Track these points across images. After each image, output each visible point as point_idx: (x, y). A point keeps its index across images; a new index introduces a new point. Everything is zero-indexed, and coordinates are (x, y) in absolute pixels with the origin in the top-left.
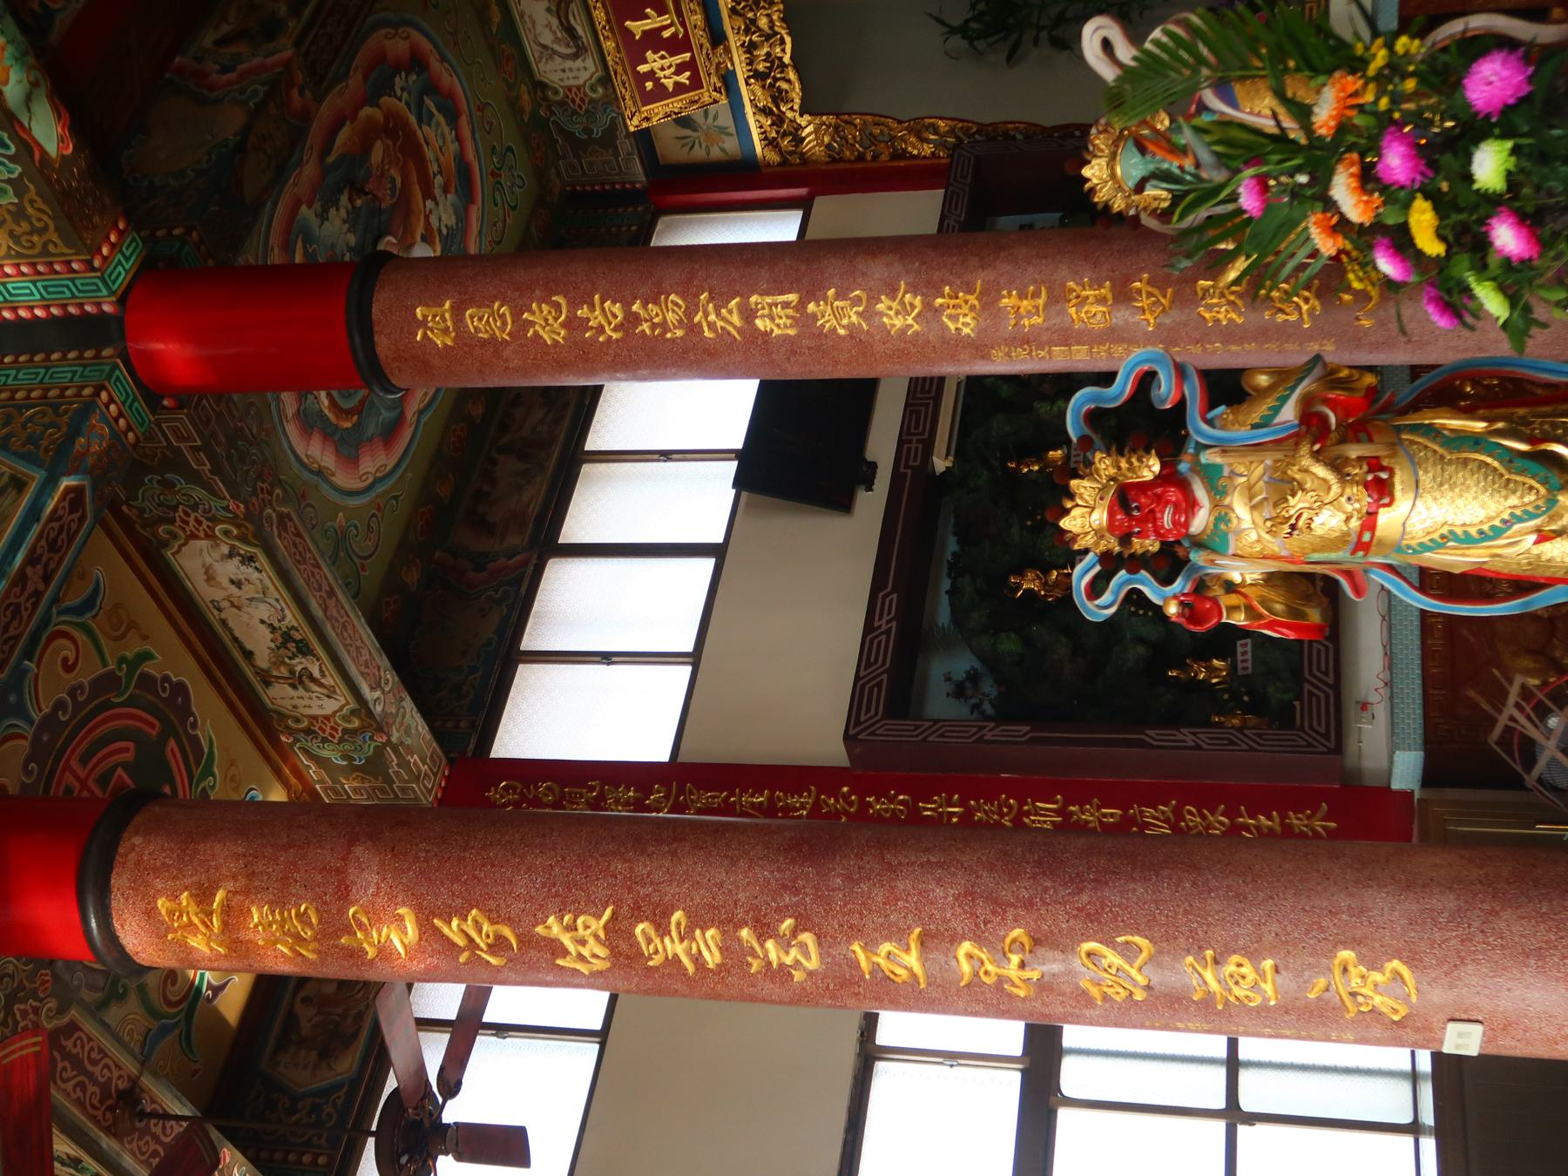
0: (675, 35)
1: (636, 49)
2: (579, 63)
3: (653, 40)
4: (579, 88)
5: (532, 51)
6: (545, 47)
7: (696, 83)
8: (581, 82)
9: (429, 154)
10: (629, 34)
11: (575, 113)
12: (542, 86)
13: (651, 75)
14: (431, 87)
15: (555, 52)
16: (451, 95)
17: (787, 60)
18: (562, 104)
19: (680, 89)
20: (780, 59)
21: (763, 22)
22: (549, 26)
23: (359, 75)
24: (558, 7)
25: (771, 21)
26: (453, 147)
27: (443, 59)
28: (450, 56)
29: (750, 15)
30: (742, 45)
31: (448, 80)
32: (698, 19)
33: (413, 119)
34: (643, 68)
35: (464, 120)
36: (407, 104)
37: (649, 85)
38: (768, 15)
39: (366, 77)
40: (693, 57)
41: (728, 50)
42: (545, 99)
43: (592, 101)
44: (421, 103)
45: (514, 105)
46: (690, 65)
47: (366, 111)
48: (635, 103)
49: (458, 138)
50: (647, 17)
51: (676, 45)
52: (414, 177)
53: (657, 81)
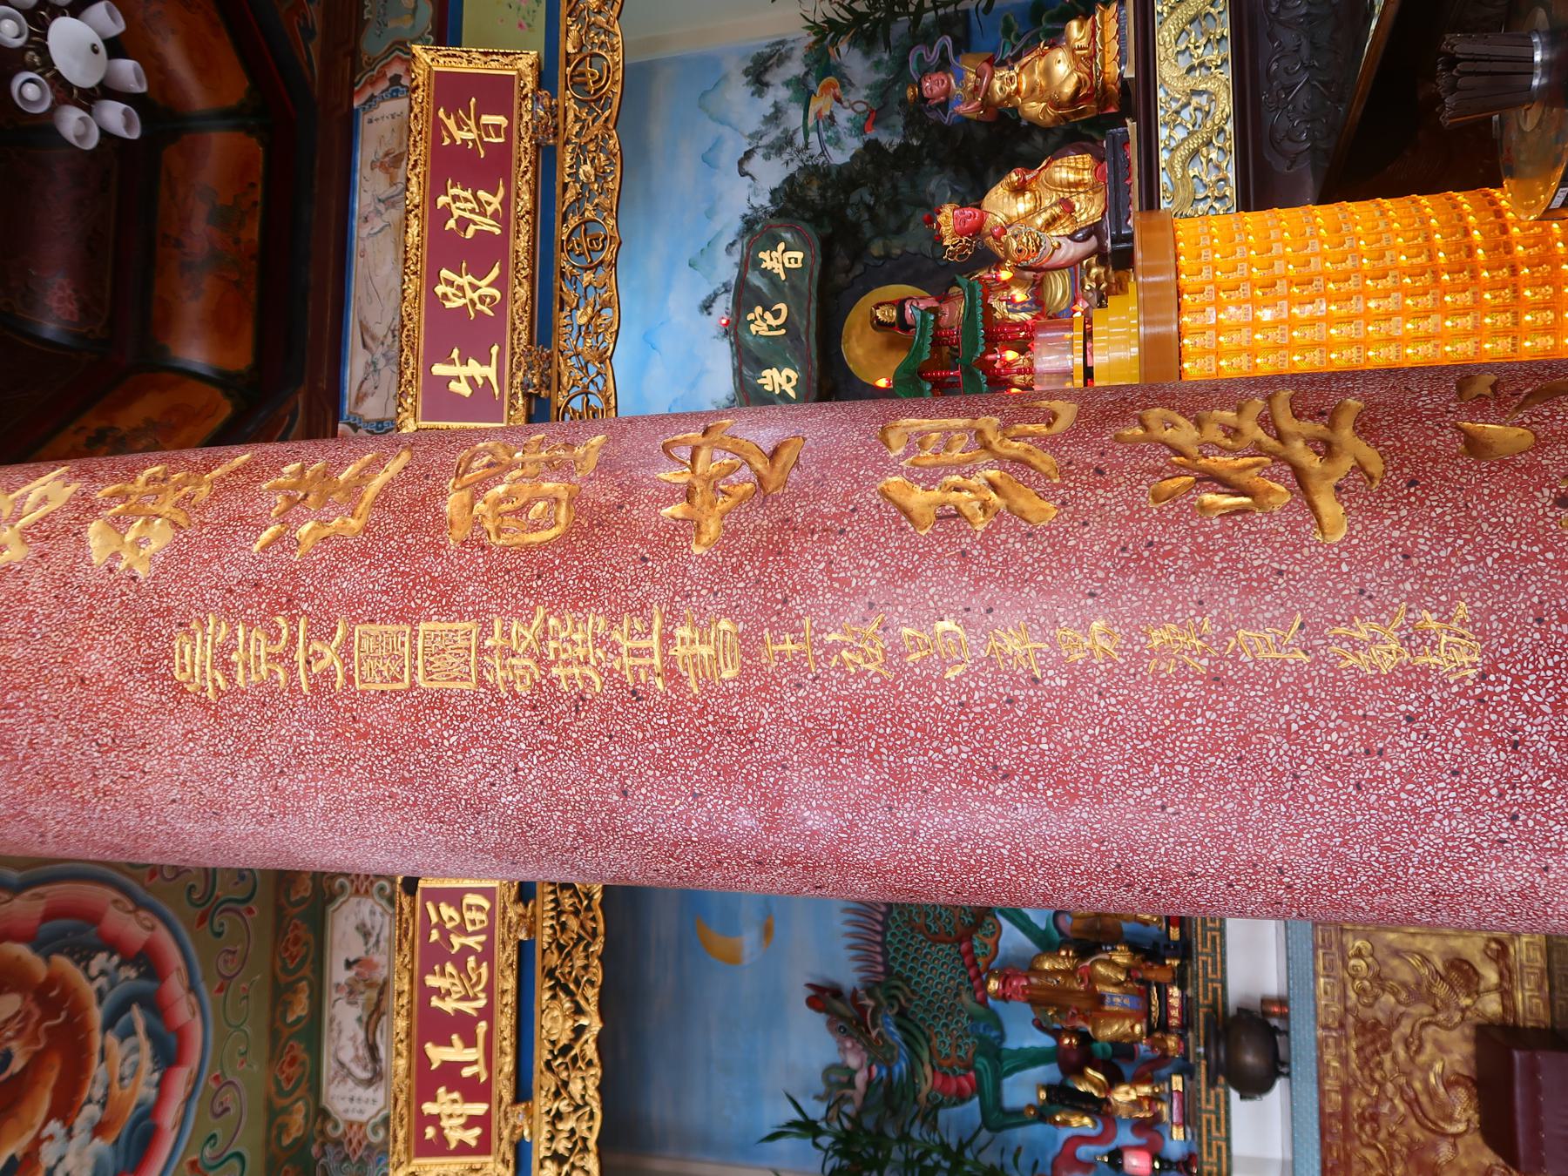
0: (476, 1077)
1: (428, 1080)
2: (369, 1093)
3: (450, 1073)
4: (361, 1125)
5: (328, 1066)
6: (342, 1065)
7: (484, 1147)
8: (364, 1118)
9: (98, 1070)
10: (424, 1060)
11: (347, 1158)
12: (323, 1114)
13: (435, 1120)
14: (156, 1006)
15: (350, 1074)
16: (181, 1034)
17: (592, 1144)
18: (338, 1143)
19: (463, 1149)
20: (585, 1140)
21: (576, 1088)
22: (353, 1039)
23: (40, 907)
24: (370, 1017)
25: (585, 1088)
26: (145, 1090)
27: (192, 988)
28: (203, 987)
29: (564, 1075)
30: (548, 1112)
31: (183, 1011)
32: (507, 1064)
33: (97, 1015)
34: (429, 1108)
35: (181, 1079)
36: (101, 994)
37: (430, 1132)
38: (583, 1079)
39: (48, 916)
40: (489, 1112)
41: (529, 1114)
42: (322, 1132)
43: (370, 1147)
44: (122, 1008)
45: (275, 1117)
46: (482, 1121)
47: (21, 950)
48: (407, 1149)
49: (162, 1086)
50: (450, 1044)
51: (474, 1090)
52: (52, 1077)
53: (440, 1130)
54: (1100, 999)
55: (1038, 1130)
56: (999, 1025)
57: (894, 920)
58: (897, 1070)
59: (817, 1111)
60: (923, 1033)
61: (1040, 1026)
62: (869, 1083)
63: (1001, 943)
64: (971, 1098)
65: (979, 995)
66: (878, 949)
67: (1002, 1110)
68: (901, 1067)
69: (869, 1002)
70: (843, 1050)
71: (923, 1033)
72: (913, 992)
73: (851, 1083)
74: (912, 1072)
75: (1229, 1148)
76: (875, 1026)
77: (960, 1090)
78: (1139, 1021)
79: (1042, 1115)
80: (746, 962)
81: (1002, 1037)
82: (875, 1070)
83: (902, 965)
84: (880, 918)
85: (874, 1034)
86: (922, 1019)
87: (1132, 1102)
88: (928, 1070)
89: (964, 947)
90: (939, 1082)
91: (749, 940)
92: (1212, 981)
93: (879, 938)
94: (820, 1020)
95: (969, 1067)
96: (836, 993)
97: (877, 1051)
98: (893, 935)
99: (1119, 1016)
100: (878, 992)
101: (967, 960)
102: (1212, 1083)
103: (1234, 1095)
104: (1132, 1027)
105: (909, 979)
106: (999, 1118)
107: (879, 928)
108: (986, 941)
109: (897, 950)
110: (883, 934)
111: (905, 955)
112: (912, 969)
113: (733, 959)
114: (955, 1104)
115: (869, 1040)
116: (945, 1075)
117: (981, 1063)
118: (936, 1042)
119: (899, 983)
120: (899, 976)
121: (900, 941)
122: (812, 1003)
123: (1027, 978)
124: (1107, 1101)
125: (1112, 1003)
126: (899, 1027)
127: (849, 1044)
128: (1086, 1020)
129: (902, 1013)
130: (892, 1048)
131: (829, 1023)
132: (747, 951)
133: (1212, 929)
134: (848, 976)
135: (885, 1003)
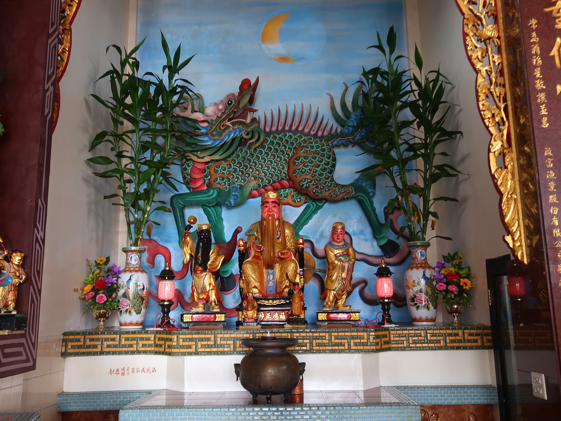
54: (270, 266)
55: (172, 229)
56: (238, 205)
57: (300, 137)
58: (206, 139)
59: (184, 73)
60: (229, 157)
61: (237, 231)
62: (195, 121)
63: (288, 206)
64: (188, 188)
65: (255, 192)
66: (280, 128)
67: (184, 207)
68: (207, 141)
69: (248, 121)
70: (216, 104)
71: (229, 157)
72: (255, 149)
73: (193, 111)
74: (206, 149)
75: (190, 354)
76: (233, 124)
77: (194, 180)
78: (260, 292)
79: (184, 230)
80: (263, 46)
81: (230, 207)
82: (206, 125)
83: (272, 143)
84: (300, 128)
85: (228, 124)
86: (238, 156)
87: (204, 287)
88: (207, 159)
89: (285, 183)
90: (199, 166)
91: (277, 48)
92: (311, 343)
93: (287, 128)
94: (236, 90)
95: (209, 186)
96: (251, 101)
97: (217, 126)
98: (290, 137)
99: (261, 279)
100: (255, 125)
101: (277, 184)
102: (246, 342)
103: (239, 359)
104: (255, 287)
105: (264, 147)
106: (177, 207)
107: (294, 128)
108: (289, 197)
109: (281, 139)
110: (290, 130)
111: (279, 144)
112: (270, 149)
113: (265, 38)
114: (184, 178)
115: (224, 120)
116: (203, 171)
117: (213, 193)
118: (224, 164)
119: (261, 140)
120: (265, 141)
121: (287, 141)
122: (246, 83)
123: (278, 219)
124: (205, 269)
125: (268, 274)
126: (234, 140)
127: (220, 107)
128: (255, 257)
129: (242, 142)
130: (220, 135)
131: (233, 95)
132: (271, 46)
133: (311, 343)
134: (265, 108)
135: (249, 130)
